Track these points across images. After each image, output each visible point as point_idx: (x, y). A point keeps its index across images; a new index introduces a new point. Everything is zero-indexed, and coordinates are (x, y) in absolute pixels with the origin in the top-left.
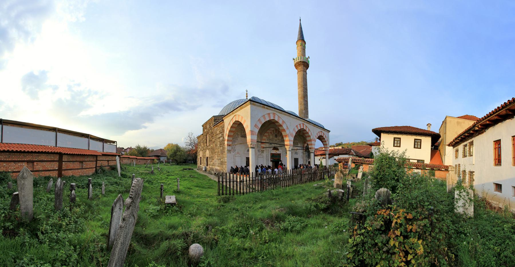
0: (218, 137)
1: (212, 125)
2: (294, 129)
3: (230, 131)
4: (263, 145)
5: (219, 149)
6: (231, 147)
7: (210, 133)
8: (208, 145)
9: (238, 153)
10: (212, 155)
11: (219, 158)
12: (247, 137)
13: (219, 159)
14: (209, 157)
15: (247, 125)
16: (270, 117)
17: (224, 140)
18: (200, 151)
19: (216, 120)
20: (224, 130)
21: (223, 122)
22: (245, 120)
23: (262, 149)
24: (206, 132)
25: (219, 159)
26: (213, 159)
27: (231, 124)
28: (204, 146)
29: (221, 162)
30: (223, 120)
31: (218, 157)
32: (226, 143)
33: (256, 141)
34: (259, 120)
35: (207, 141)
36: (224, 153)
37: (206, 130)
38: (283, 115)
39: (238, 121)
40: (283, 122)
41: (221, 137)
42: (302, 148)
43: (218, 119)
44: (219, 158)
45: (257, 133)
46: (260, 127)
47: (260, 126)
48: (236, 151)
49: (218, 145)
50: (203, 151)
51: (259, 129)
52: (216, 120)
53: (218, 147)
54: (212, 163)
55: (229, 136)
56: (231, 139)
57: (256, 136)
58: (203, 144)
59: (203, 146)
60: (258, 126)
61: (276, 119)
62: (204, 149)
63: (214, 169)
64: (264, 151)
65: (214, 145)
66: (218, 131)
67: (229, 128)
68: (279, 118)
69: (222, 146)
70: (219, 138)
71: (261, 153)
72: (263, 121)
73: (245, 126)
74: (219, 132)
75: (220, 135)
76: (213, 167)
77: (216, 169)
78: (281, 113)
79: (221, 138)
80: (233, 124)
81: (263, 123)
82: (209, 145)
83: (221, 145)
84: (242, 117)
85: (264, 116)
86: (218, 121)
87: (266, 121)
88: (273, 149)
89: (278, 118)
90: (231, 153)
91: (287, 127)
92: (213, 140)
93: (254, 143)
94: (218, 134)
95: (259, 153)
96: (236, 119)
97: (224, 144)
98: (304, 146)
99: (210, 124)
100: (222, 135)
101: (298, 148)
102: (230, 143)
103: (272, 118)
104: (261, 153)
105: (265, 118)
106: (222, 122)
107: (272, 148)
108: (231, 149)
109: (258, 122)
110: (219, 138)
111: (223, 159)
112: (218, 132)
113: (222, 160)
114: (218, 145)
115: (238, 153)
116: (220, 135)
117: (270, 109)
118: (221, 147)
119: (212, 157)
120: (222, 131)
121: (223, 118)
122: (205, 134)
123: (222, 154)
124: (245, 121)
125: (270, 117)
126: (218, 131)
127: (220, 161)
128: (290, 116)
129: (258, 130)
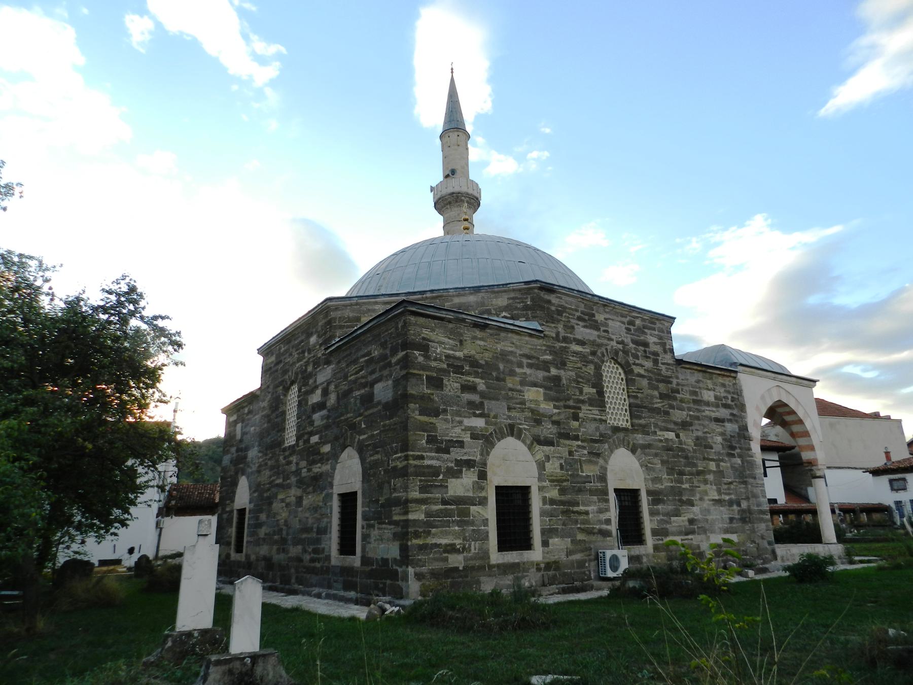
0: (713, 415)
5: (722, 460)
10: (682, 483)
11: (727, 498)
13: (731, 503)
14: (649, 493)
18: (488, 440)
25: (731, 503)
26: (691, 503)
29: (743, 511)
31: (719, 492)
36: (751, 480)
44: (727, 498)
49: (718, 448)
53: (719, 453)
54: (680, 521)
63: (704, 547)
65: (688, 440)
66: (712, 393)
69: (740, 456)
74: (716, 397)
76: (695, 539)
77: (713, 546)
79: (731, 427)
83: (732, 448)
97: (750, 449)
111: (752, 501)
113: (744, 505)
119: (677, 492)
123: (745, 483)
127: (735, 507)
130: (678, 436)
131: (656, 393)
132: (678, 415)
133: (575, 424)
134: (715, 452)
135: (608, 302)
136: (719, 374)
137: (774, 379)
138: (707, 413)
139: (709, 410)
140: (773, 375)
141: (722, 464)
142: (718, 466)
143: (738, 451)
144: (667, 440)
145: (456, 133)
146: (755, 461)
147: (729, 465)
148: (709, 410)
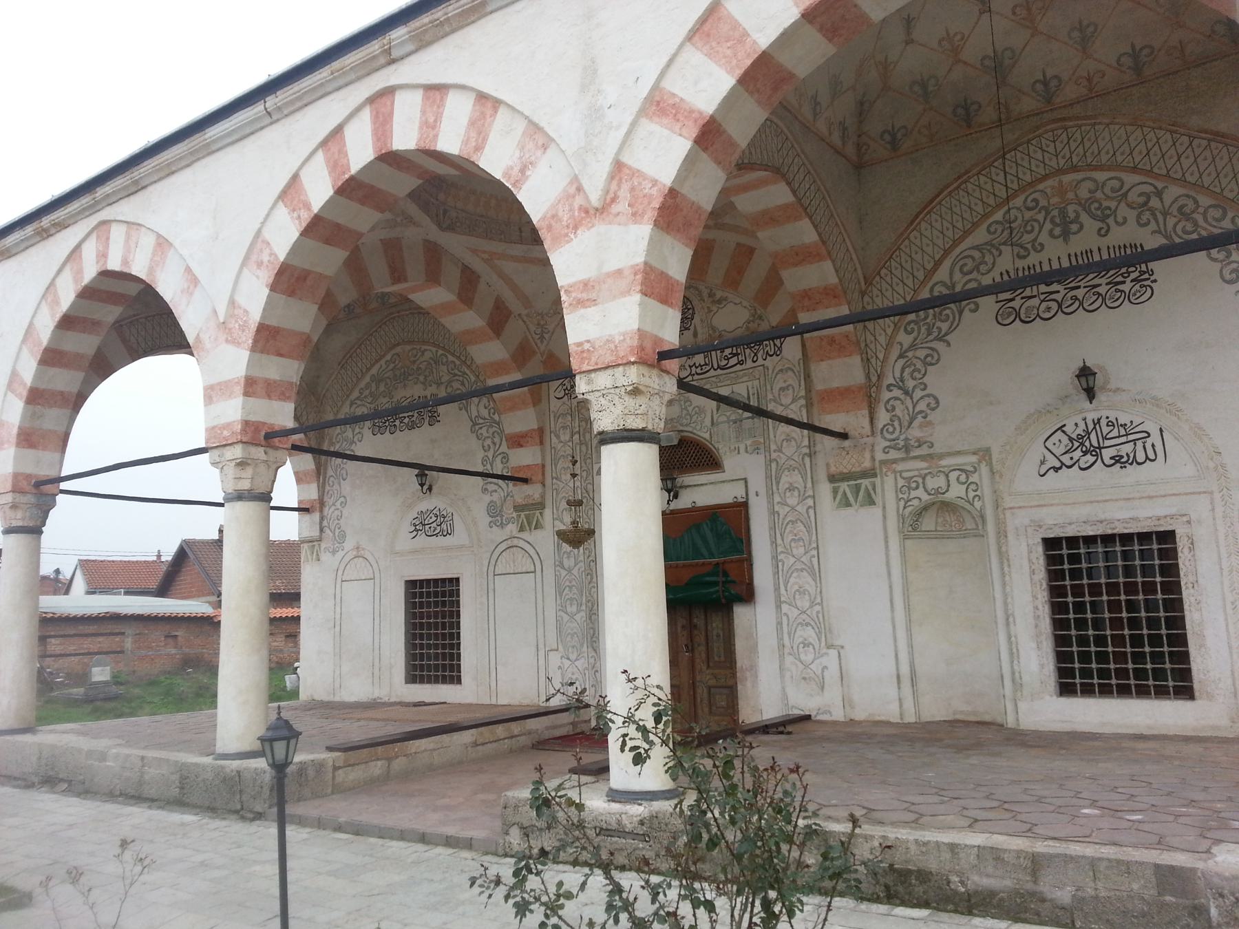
9: (359, 553)
23: (521, 493)
48: (349, 544)
64: (541, 506)
71: (512, 528)
90: (325, 557)
91: (188, 270)
95: (498, 534)
104: (512, 528)
115: (359, 553)
128: (209, 150)
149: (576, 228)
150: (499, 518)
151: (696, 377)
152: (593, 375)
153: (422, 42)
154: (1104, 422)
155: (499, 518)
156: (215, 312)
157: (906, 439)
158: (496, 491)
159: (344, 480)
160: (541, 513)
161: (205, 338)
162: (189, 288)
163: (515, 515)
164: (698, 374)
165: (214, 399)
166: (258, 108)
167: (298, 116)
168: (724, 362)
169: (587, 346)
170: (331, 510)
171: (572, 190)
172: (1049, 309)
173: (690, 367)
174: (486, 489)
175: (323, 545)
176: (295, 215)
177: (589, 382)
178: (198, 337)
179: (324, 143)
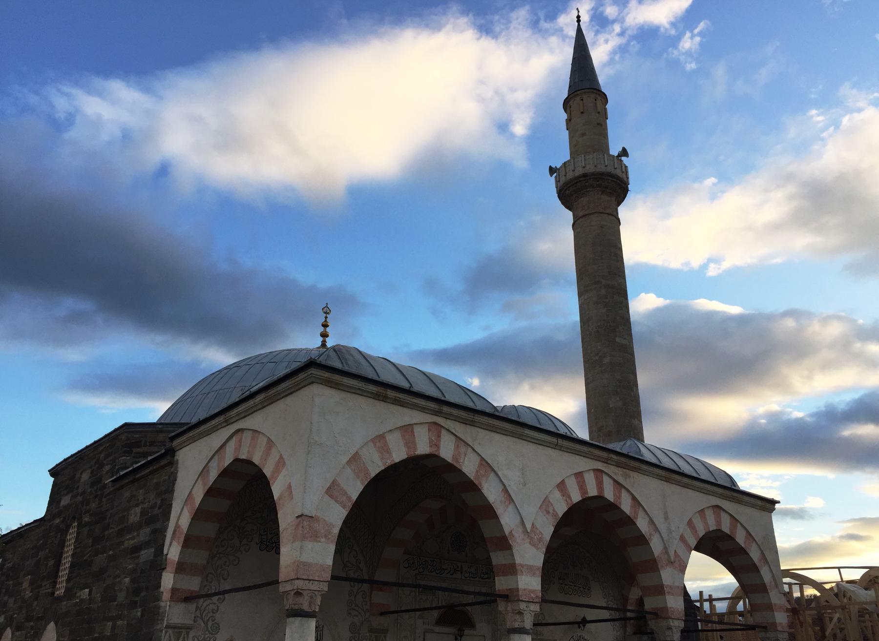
1: (112, 472)
2: (546, 505)
3: (199, 515)
4: (381, 598)
5: (119, 617)
6: (192, 607)
7: (86, 519)
8: (60, 592)
12: (284, 550)
15: (289, 487)
16: (410, 443)
17: (158, 565)
19: (138, 444)
20: (170, 506)
21: (173, 463)
22: (281, 457)
24: (67, 507)
27: (213, 475)
28: (36, 599)
30: (171, 453)
32: (168, 580)
33: (327, 576)
34: (355, 459)
35: (58, 563)
37: (65, 501)
38: (482, 434)
39: (249, 463)
40: (485, 465)
41: (147, 545)
42: (616, 615)
43: (152, 444)
45: (336, 531)
46: (355, 496)
47: (355, 489)
49: (121, 597)
50: (18, 628)
51: (350, 505)
52: (138, 444)
55: (189, 542)
56: (200, 557)
57: (332, 547)
58: (32, 583)
59: (28, 594)
60: (345, 493)
61: (447, 452)
62: (29, 618)
64: (385, 631)
66: (138, 510)
67: (199, 495)
68: (463, 449)
70: (136, 549)
72: (376, 466)
73: (276, 490)
74: (143, 513)
75: (144, 534)
78: (472, 423)
79: (146, 554)
80: (225, 473)
81: (373, 475)
82: (68, 590)
84: (270, 444)
85: (381, 437)
86: (145, 455)
87: (389, 463)
88: (440, 622)
89: (457, 447)
91: (506, 490)
92: (100, 560)
93: (314, 586)
94: (130, 529)
96: (238, 448)
98: (625, 599)
99: (102, 466)
100: (154, 532)
101: (591, 614)
102: (193, 584)
103: (423, 448)
105: (385, 450)
106: (164, 462)
107: (435, 614)
108: (188, 621)
109: (348, 470)
110: (136, 549)
112: (135, 516)
114: (121, 597)
116: (144, 534)
117: (414, 407)
118: (133, 605)
120: (156, 511)
121: (175, 443)
122: (57, 521)
124: (281, 463)
125: (410, 443)
126: (138, 510)
128: (521, 437)
129: (344, 513)
130: (90, 593)
131: (90, 541)
132: (100, 560)
133: (36, 603)
134: (117, 605)
135: (80, 453)
136: (151, 473)
137: (228, 423)
138: (126, 544)
139: (130, 539)
140: (221, 418)
141: (119, 623)
142: (114, 627)
143: (143, 594)
144: (82, 600)
145: (593, 96)
146: (159, 607)
147: (125, 622)
148: (130, 539)
149: (666, 565)
150: (357, 635)
151: (471, 579)
152: (674, 620)
153: (618, 465)
154: (582, 637)
155: (357, 635)
156: (523, 523)
157: (537, 630)
158: (357, 616)
159: (225, 579)
160: (385, 637)
161: (516, 535)
162: (505, 502)
163: (368, 634)
164: (473, 578)
165: (524, 573)
166: (554, 440)
167: (566, 454)
168: (482, 576)
169: (673, 610)
170: (205, 604)
171: (664, 551)
172: (570, 591)
173: (469, 573)
174: (350, 613)
175: (192, 634)
176: (564, 498)
177: (673, 622)
178: (511, 532)
179: (576, 474)
